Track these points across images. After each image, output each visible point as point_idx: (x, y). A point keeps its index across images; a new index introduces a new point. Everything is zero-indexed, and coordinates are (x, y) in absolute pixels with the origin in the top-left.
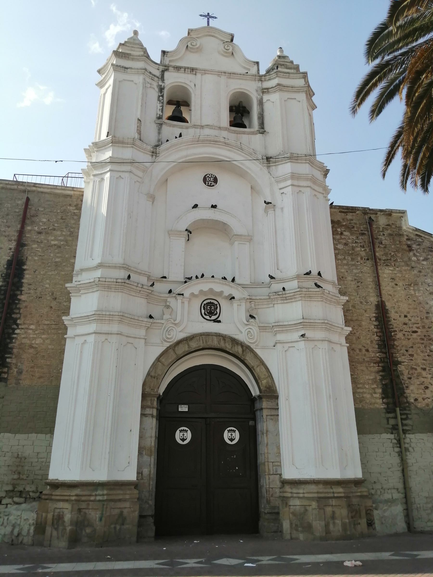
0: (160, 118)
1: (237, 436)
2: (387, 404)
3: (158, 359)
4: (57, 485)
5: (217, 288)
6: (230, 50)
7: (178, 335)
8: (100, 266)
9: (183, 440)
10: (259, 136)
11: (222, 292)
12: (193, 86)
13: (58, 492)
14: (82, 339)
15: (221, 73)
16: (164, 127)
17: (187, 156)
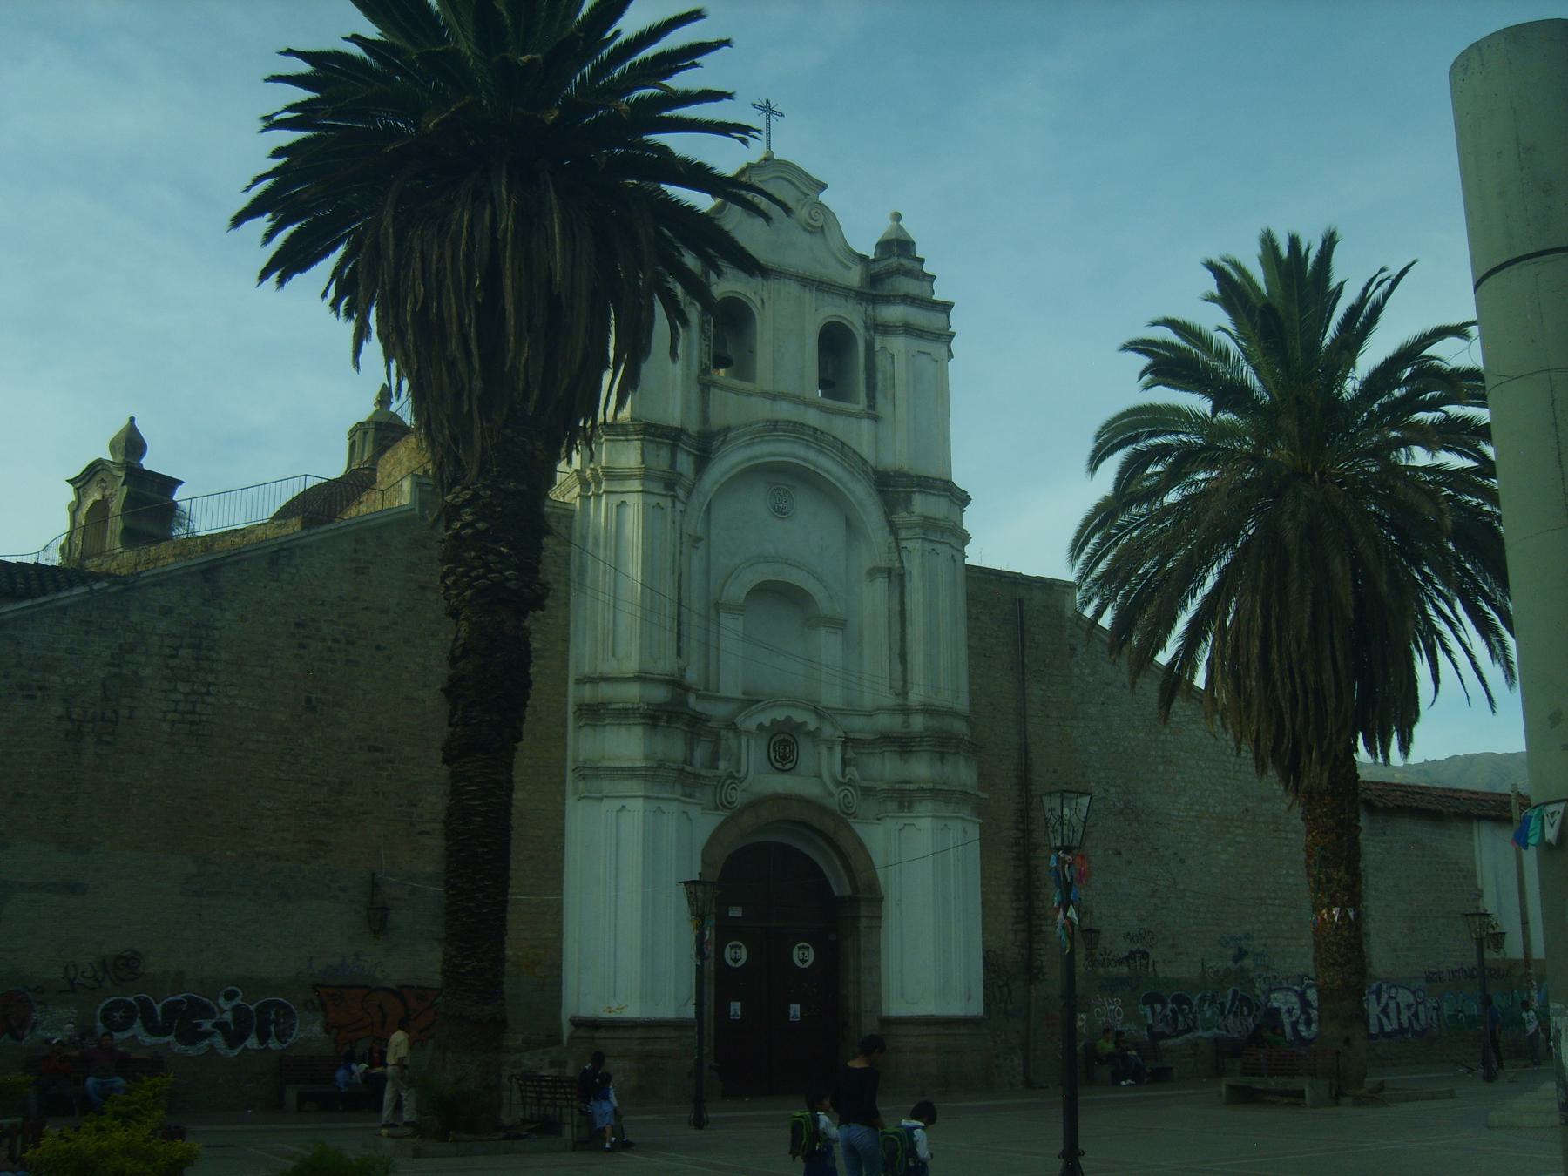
0: (705, 371)
1: (811, 955)
2: (1017, 910)
3: (714, 838)
4: (594, 1025)
5: (799, 716)
6: (818, 224)
7: (739, 798)
8: (642, 678)
9: (736, 961)
10: (866, 424)
11: (805, 723)
12: (759, 303)
13: (601, 1034)
14: (617, 804)
15: (807, 282)
16: (715, 393)
17: (750, 459)
